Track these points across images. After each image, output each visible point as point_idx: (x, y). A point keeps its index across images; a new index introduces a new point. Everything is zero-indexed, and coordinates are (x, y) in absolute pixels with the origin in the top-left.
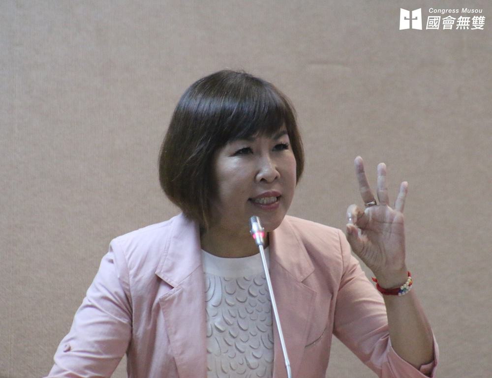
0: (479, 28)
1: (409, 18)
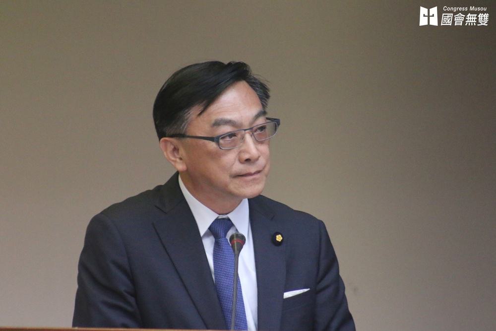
0: (484, 24)
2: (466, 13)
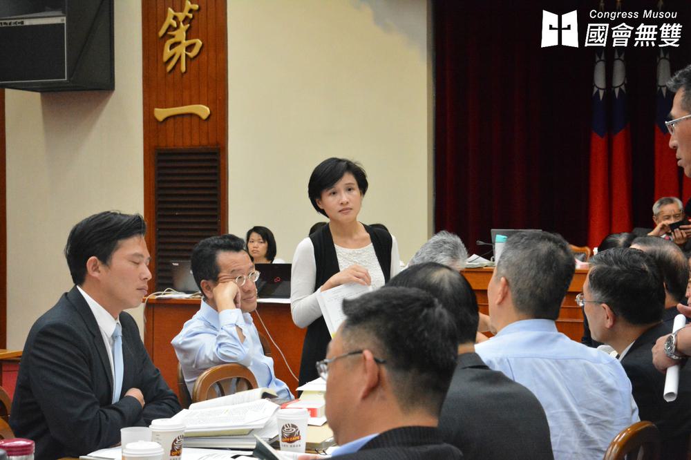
0: (672, 44)
1: (557, 27)
2: (634, 23)
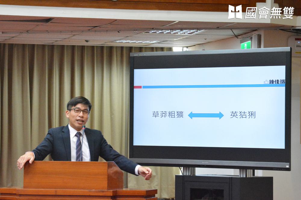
0: (289, 17)
